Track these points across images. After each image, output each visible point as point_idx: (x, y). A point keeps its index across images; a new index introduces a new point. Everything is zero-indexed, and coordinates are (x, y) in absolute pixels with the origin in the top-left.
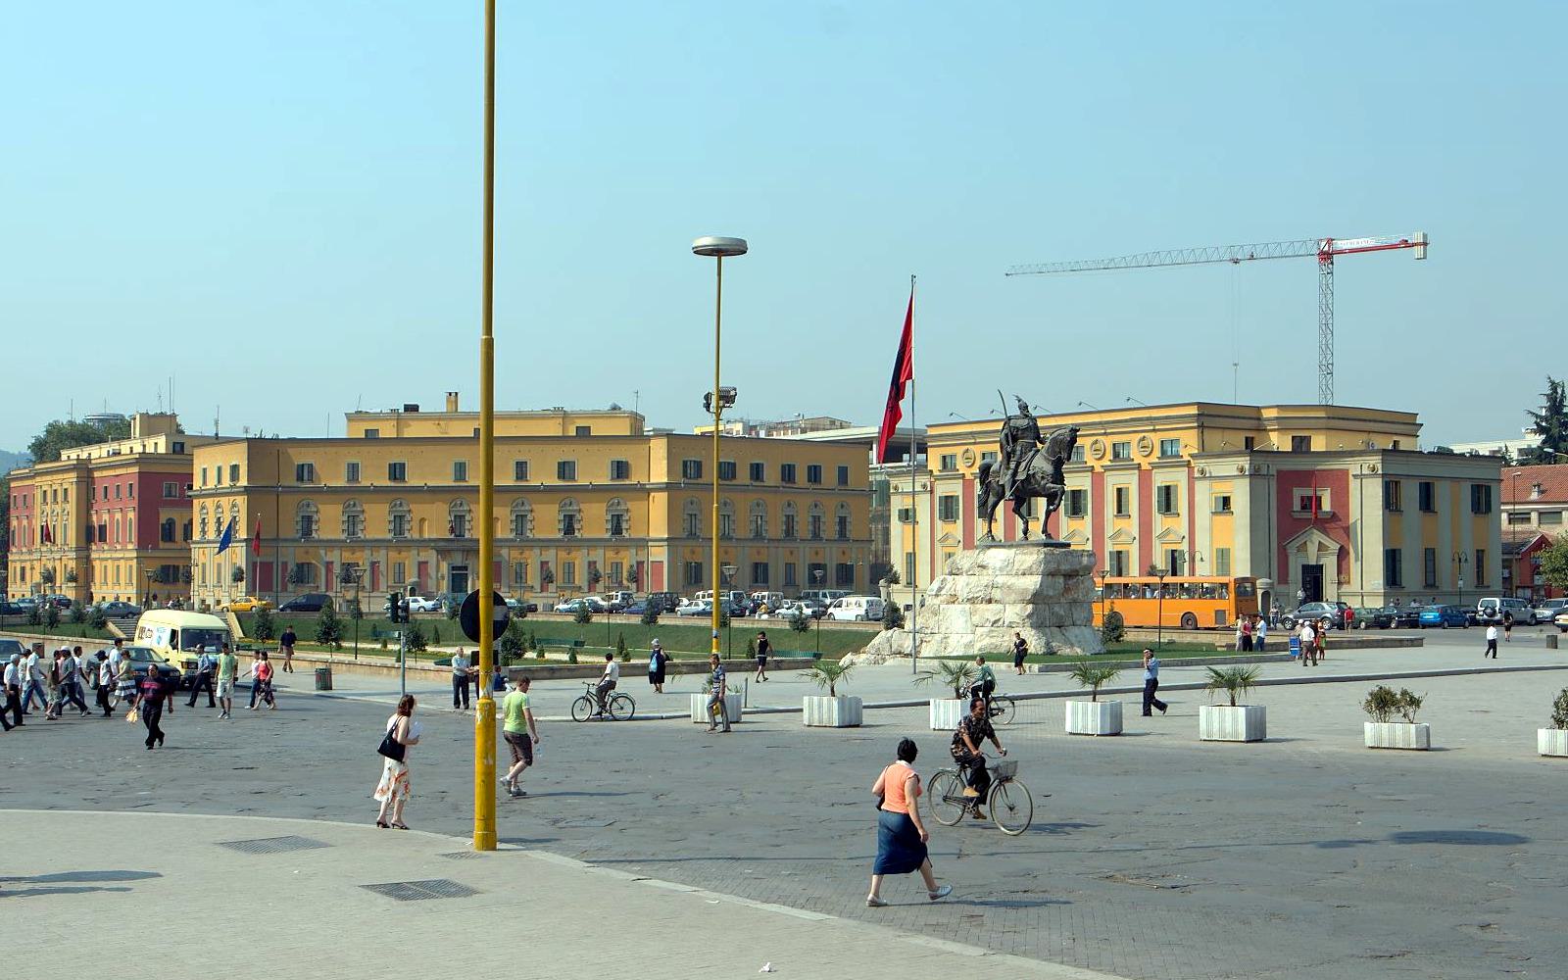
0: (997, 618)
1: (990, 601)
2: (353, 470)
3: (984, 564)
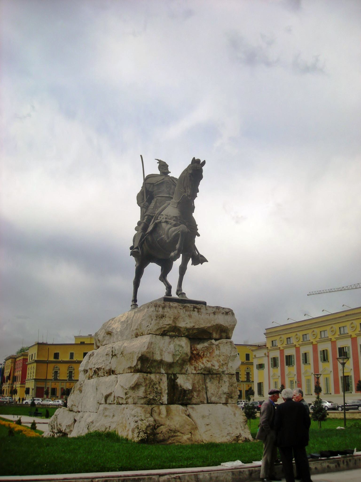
1: (111, 372)
2: (72, 355)
3: (110, 329)
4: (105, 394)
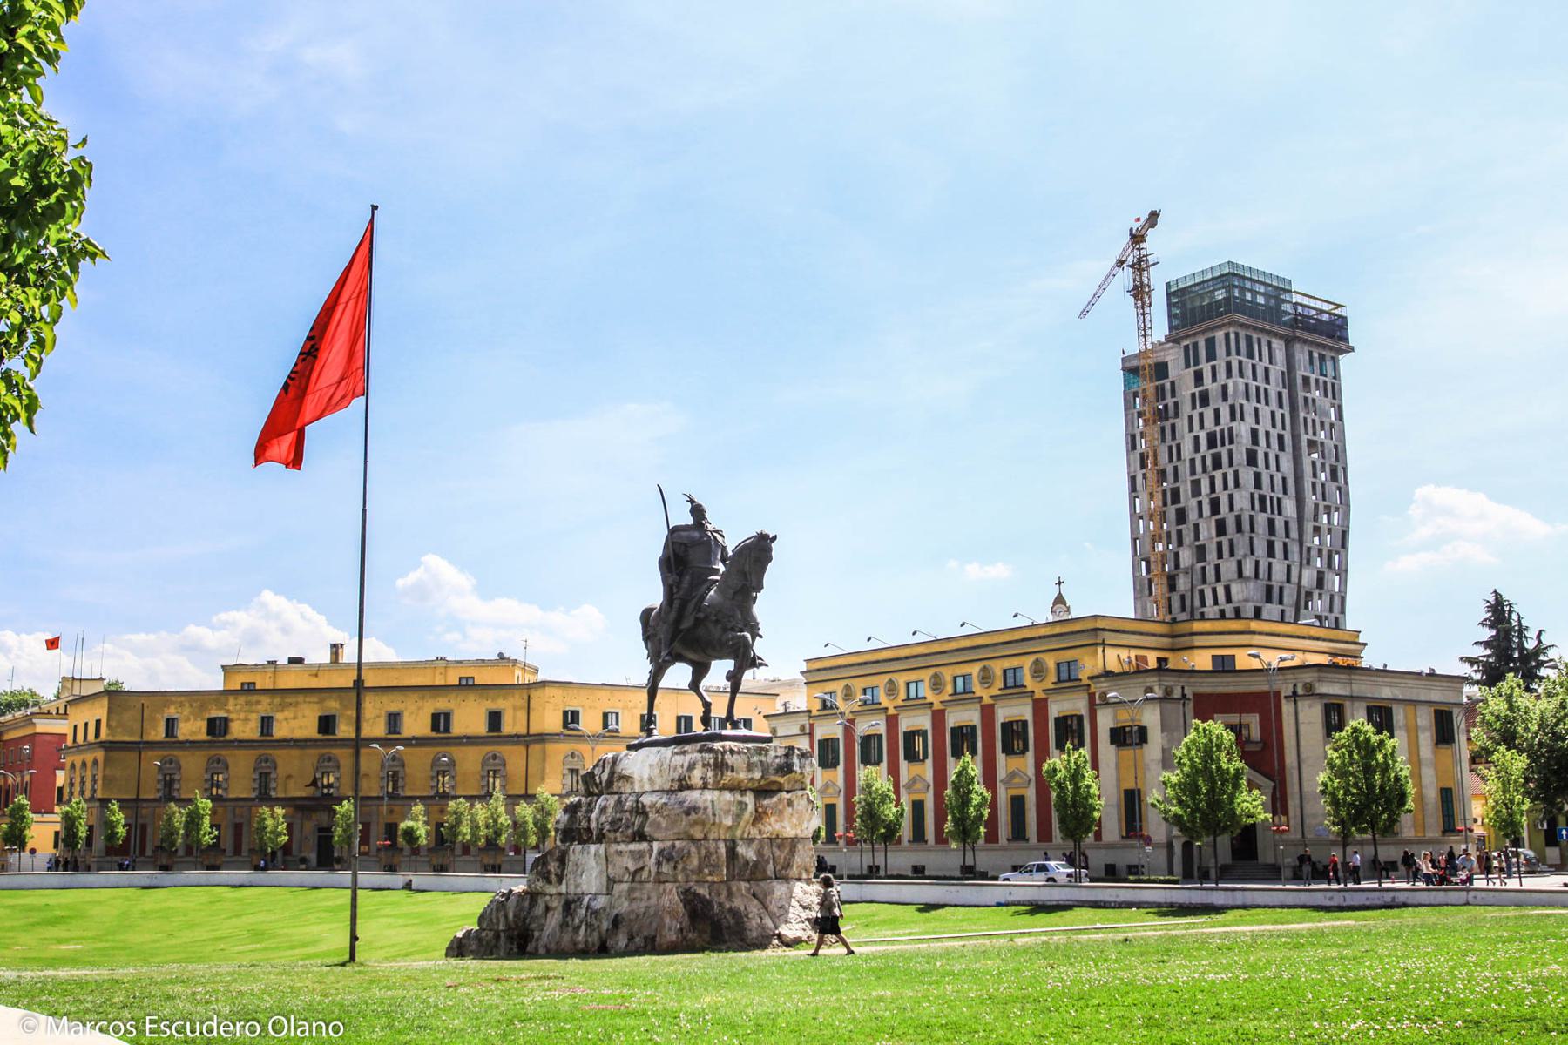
0: (641, 864)
4: (632, 869)
